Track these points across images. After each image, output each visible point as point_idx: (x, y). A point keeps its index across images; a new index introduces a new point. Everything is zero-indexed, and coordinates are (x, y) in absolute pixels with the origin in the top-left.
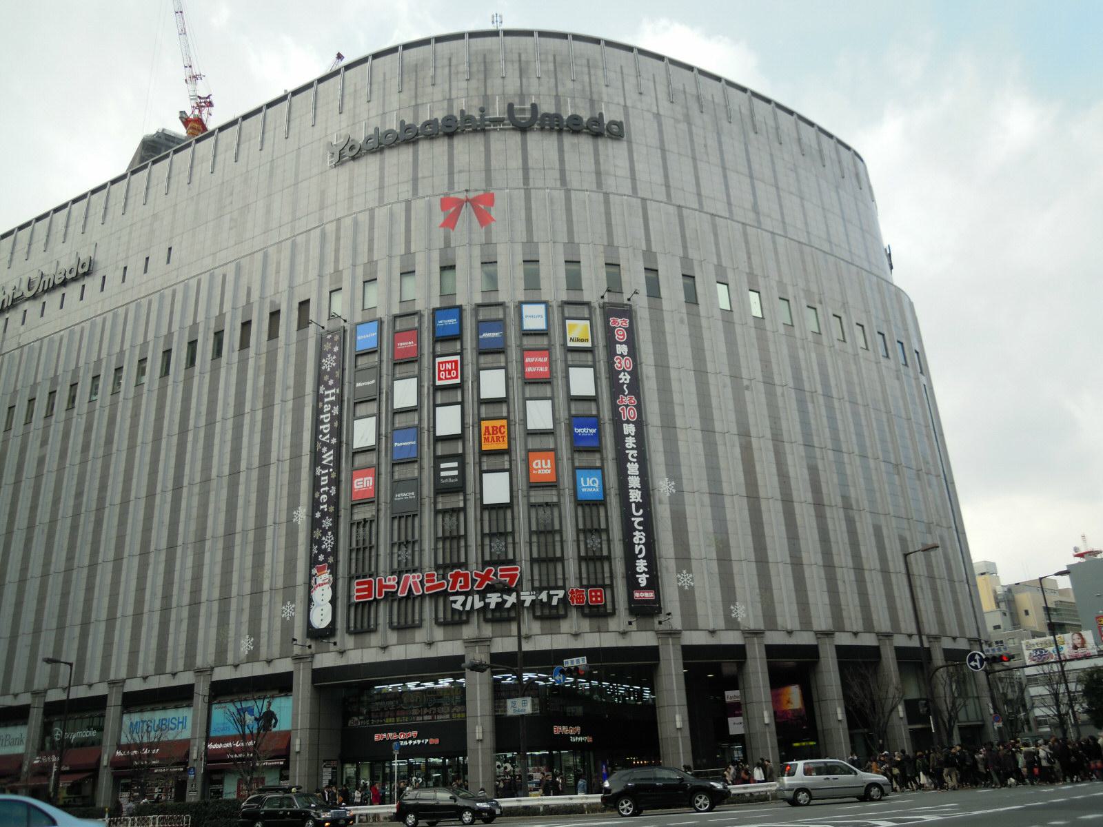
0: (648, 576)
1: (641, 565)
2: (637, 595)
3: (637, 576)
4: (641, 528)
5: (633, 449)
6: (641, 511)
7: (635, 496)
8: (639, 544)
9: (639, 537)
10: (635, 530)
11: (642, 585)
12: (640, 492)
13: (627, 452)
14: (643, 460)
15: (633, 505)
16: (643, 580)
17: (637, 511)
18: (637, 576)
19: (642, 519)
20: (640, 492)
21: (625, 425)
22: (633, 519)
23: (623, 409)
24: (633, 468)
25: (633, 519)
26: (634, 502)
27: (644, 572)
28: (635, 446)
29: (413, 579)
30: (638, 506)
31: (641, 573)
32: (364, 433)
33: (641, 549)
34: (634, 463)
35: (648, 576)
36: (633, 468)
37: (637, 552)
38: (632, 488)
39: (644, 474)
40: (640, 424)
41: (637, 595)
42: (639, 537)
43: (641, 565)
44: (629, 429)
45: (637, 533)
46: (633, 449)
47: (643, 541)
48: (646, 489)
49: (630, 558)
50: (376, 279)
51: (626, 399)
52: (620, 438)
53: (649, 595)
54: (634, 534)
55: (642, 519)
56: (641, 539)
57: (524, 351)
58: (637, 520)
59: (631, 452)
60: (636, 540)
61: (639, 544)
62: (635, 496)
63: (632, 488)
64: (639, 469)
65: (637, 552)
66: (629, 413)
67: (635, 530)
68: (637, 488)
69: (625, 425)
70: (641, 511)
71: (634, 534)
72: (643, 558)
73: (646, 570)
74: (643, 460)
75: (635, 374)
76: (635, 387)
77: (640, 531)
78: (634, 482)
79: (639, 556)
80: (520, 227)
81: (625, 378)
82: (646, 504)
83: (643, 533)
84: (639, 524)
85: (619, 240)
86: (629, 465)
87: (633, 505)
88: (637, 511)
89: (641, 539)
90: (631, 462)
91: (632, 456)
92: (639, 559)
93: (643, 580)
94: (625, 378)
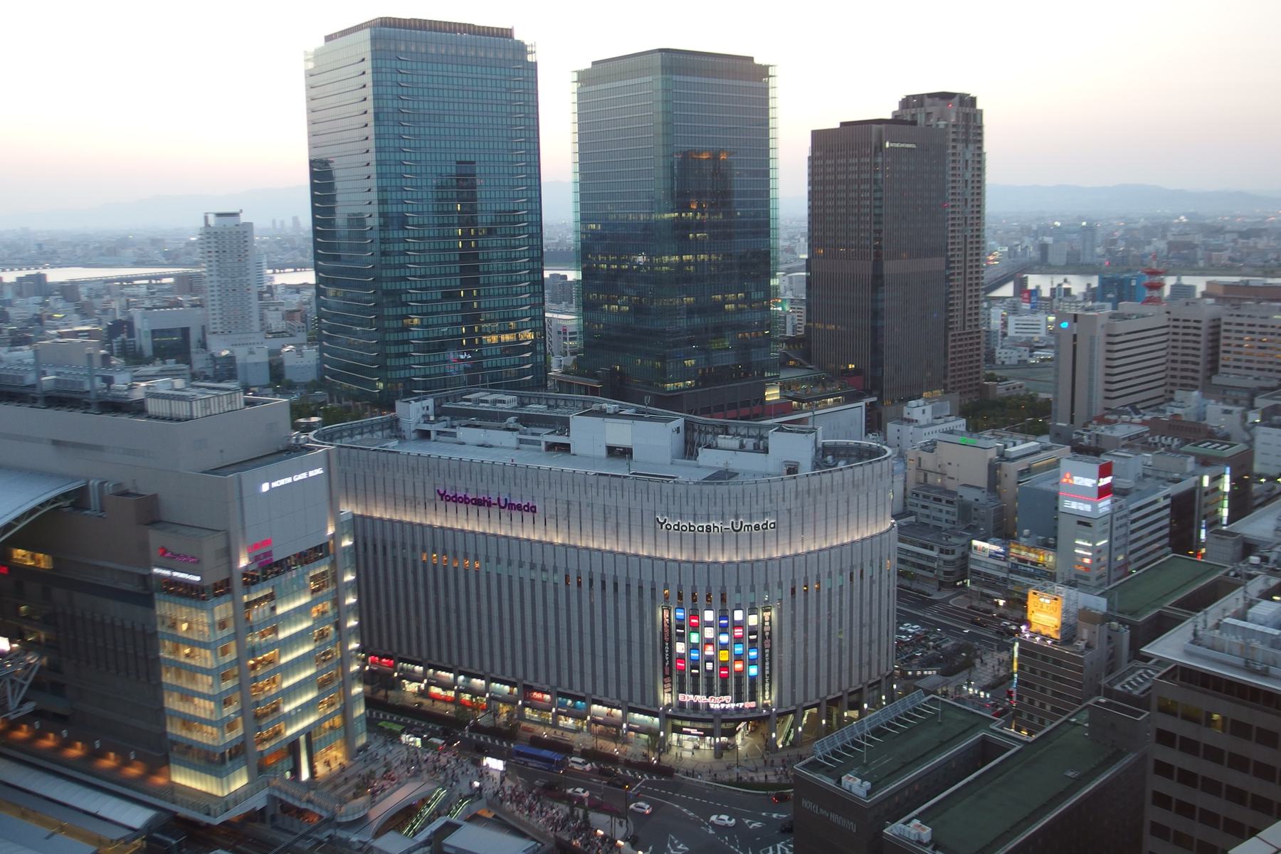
1: (767, 693)
7: (767, 672)
9: (767, 685)
14: (770, 661)
16: (767, 697)
24: (767, 664)
29: (698, 697)
32: (680, 648)
36: (767, 664)
39: (770, 666)
40: (770, 649)
42: (767, 685)
43: (767, 693)
44: (767, 651)
48: (770, 670)
49: (764, 691)
51: (767, 641)
52: (764, 654)
57: (734, 627)
62: (767, 672)
66: (767, 646)
74: (770, 661)
75: (770, 632)
76: (770, 637)
78: (767, 668)
80: (735, 580)
81: (767, 634)
82: (770, 675)
85: (770, 580)
93: (767, 697)
94: (767, 634)
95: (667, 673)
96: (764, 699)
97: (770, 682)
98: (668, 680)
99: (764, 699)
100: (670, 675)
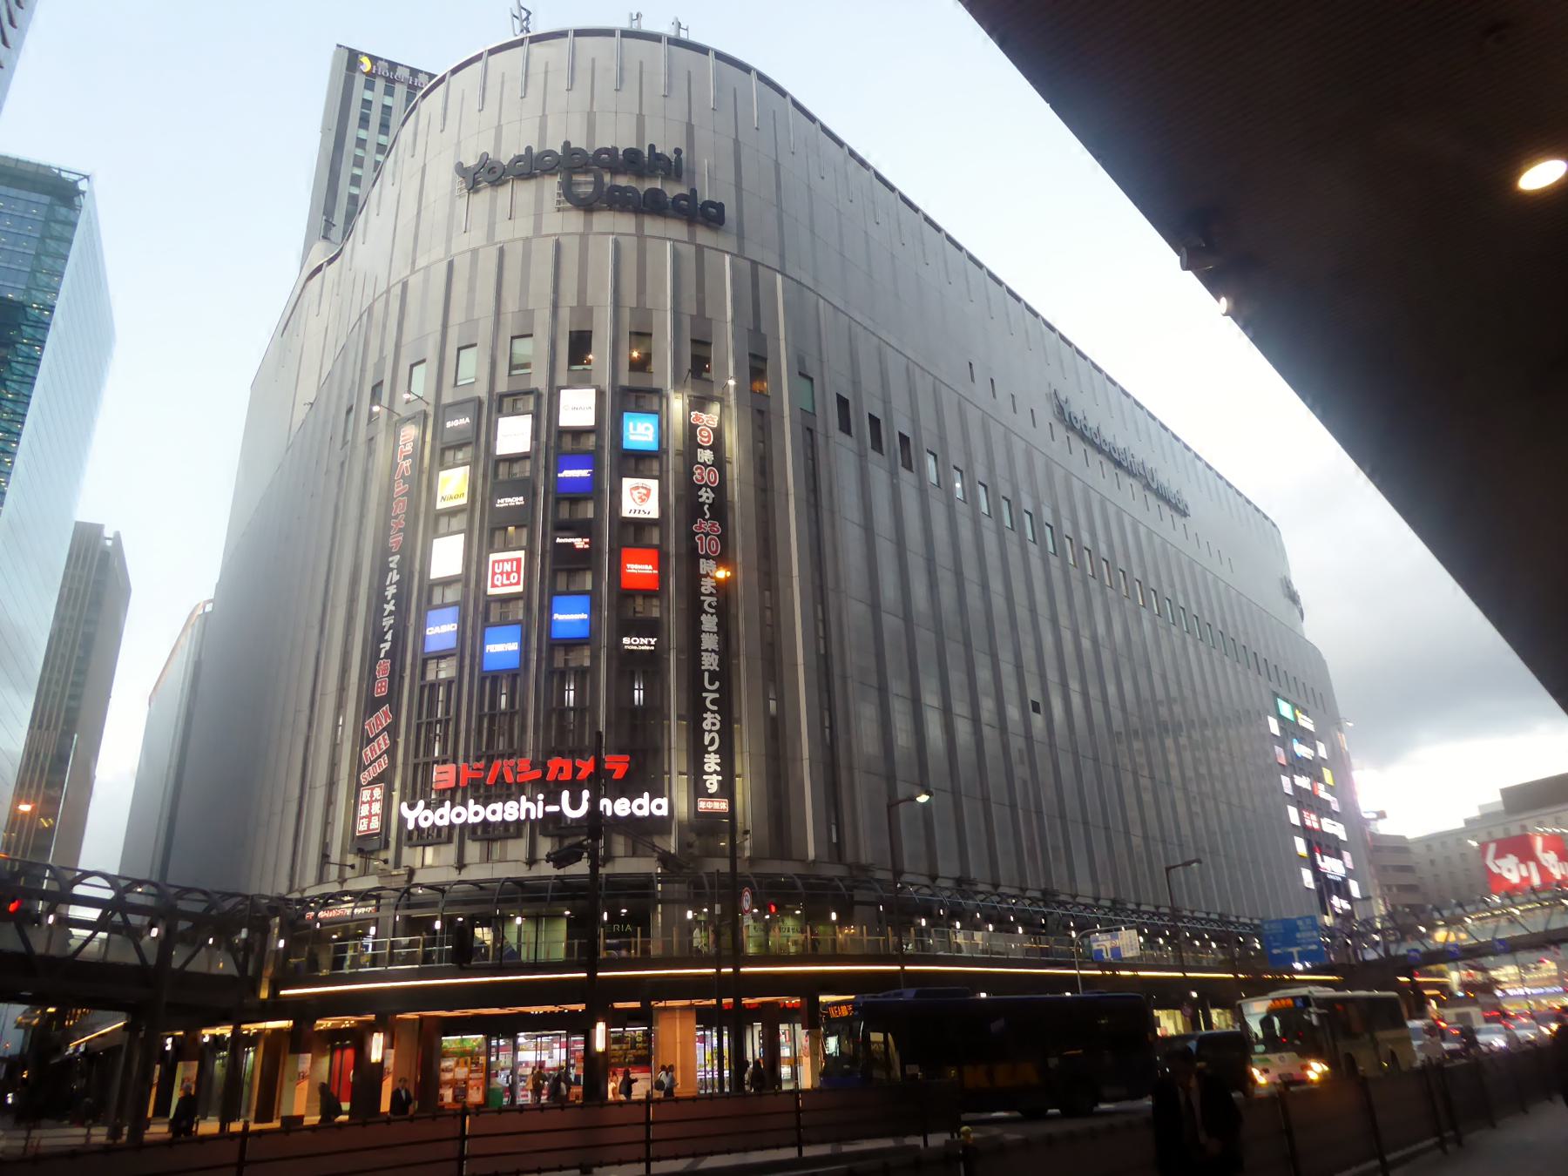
0: (720, 778)
1: (712, 762)
2: (703, 805)
3: (705, 777)
4: (715, 708)
5: (711, 594)
6: (717, 684)
7: (710, 662)
8: (710, 731)
9: (711, 721)
10: (707, 710)
11: (709, 791)
12: (717, 657)
13: (702, 598)
15: (706, 674)
16: (713, 783)
17: (711, 683)
18: (705, 777)
19: (717, 695)
20: (717, 657)
21: (701, 560)
22: (704, 695)
23: (700, 539)
25: (704, 695)
26: (708, 670)
27: (715, 772)
28: (714, 592)
30: (714, 677)
31: (711, 774)
33: (712, 742)
34: (712, 614)
35: (720, 778)
37: (706, 743)
38: (707, 650)
39: (725, 631)
41: (703, 805)
42: (711, 721)
43: (712, 762)
45: (708, 715)
46: (711, 594)
47: (717, 727)
48: (726, 651)
49: (697, 753)
50: (382, 382)
53: (721, 805)
54: (705, 715)
55: (717, 695)
56: (714, 724)
58: (710, 696)
59: (708, 600)
60: (706, 725)
61: (710, 731)
62: (710, 662)
63: (707, 650)
64: (717, 624)
65: (706, 743)
67: (707, 710)
68: (713, 651)
69: (701, 560)
70: (717, 684)
71: (705, 715)
72: (715, 752)
73: (718, 769)
77: (713, 712)
78: (709, 641)
79: (710, 749)
82: (724, 675)
83: (717, 715)
84: (713, 702)
86: (704, 618)
87: (706, 674)
88: (711, 683)
89: (714, 724)
90: (707, 613)
91: (710, 605)
92: (709, 753)
95: (381, 690)
96: (699, 790)
97: (726, 707)
98: (383, 717)
99: (699, 790)
100: (392, 698)
